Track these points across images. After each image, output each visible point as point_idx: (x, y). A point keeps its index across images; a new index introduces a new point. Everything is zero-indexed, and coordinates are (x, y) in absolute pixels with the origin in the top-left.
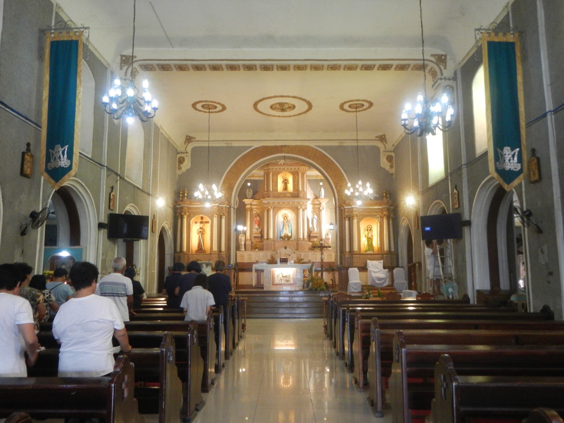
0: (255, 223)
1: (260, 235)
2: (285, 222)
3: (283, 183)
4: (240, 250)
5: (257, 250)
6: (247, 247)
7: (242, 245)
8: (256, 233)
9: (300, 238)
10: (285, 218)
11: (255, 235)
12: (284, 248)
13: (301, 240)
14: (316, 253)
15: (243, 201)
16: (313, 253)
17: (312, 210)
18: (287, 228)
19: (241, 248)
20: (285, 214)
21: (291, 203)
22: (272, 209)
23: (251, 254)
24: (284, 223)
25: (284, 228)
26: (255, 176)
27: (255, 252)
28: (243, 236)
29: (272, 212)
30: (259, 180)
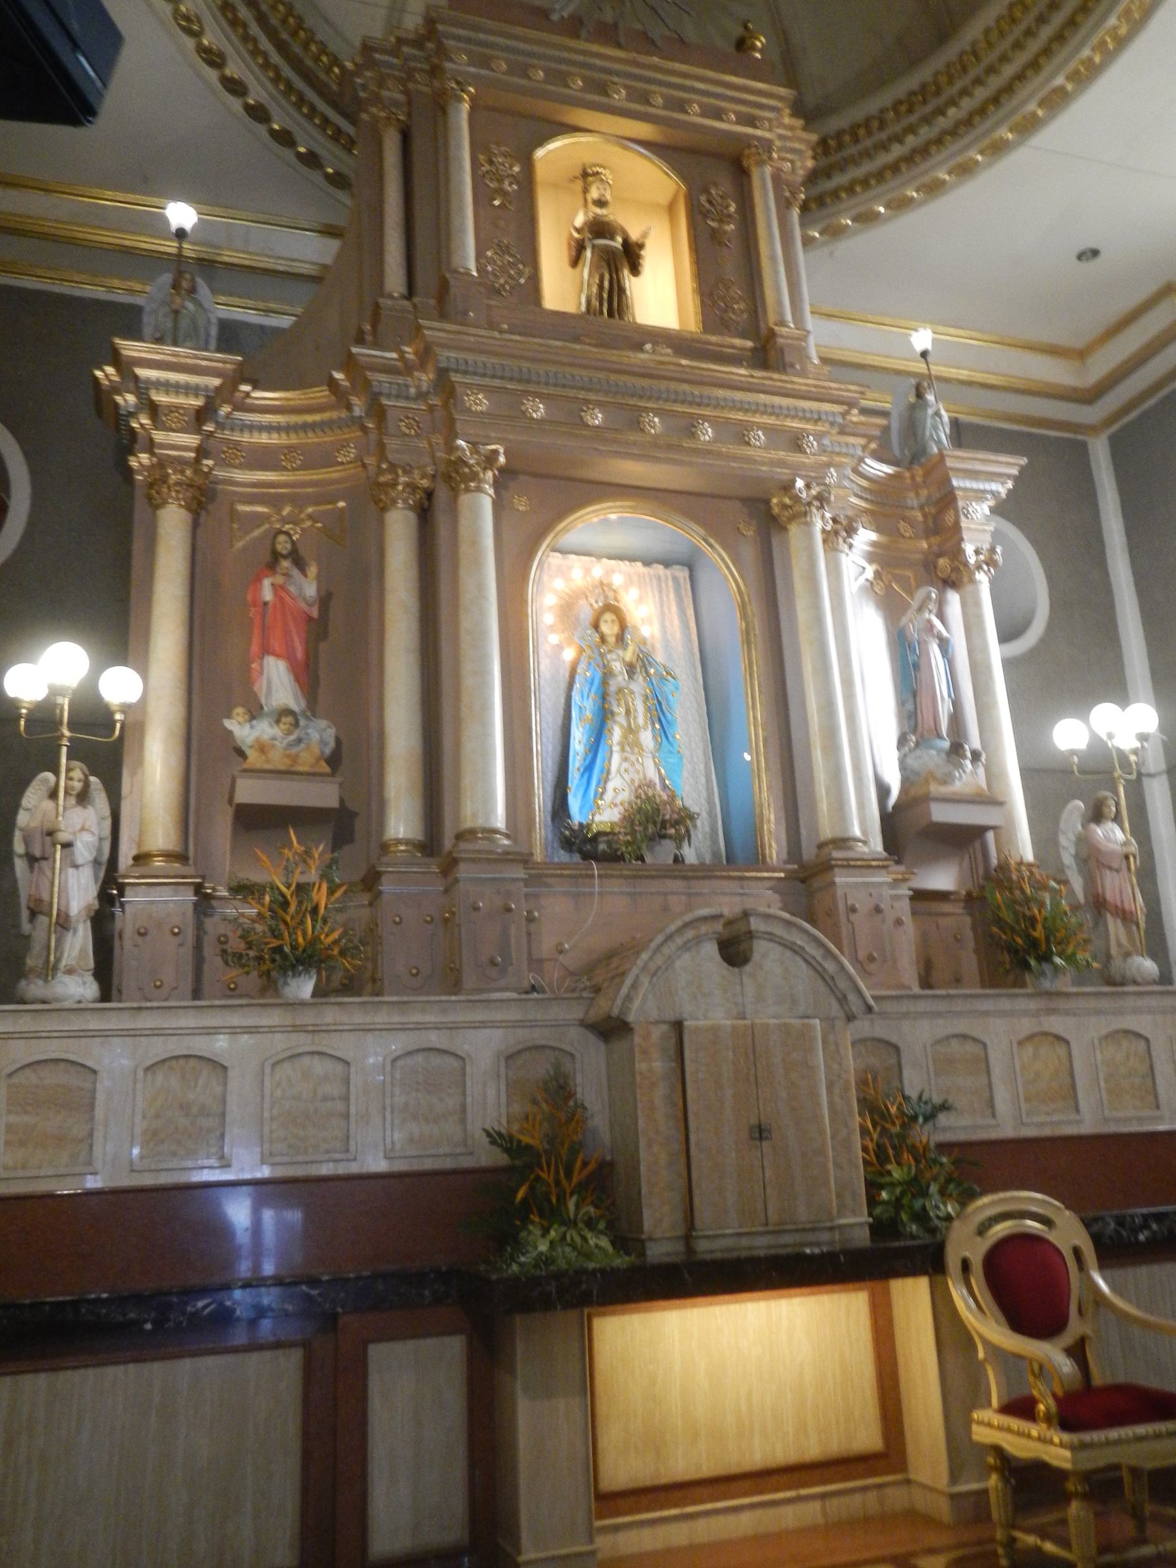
0: (266, 650)
1: (325, 795)
2: (617, 666)
3: (575, 261)
4: (34, 988)
5: (304, 987)
6: (127, 952)
7: (64, 924)
8: (277, 760)
9: (843, 842)
10: (609, 628)
11: (250, 792)
12: (711, 949)
13: (865, 865)
14: (1055, 1024)
15: (107, 374)
16: (1026, 1026)
17: (870, 572)
18: (647, 738)
19: (49, 970)
20: (603, 586)
21: (707, 433)
22: (489, 475)
23: (199, 1045)
24: (607, 675)
25: (617, 734)
26: (228, 256)
27: (273, 1018)
28: (83, 798)
29: (486, 503)
30: (262, 328)
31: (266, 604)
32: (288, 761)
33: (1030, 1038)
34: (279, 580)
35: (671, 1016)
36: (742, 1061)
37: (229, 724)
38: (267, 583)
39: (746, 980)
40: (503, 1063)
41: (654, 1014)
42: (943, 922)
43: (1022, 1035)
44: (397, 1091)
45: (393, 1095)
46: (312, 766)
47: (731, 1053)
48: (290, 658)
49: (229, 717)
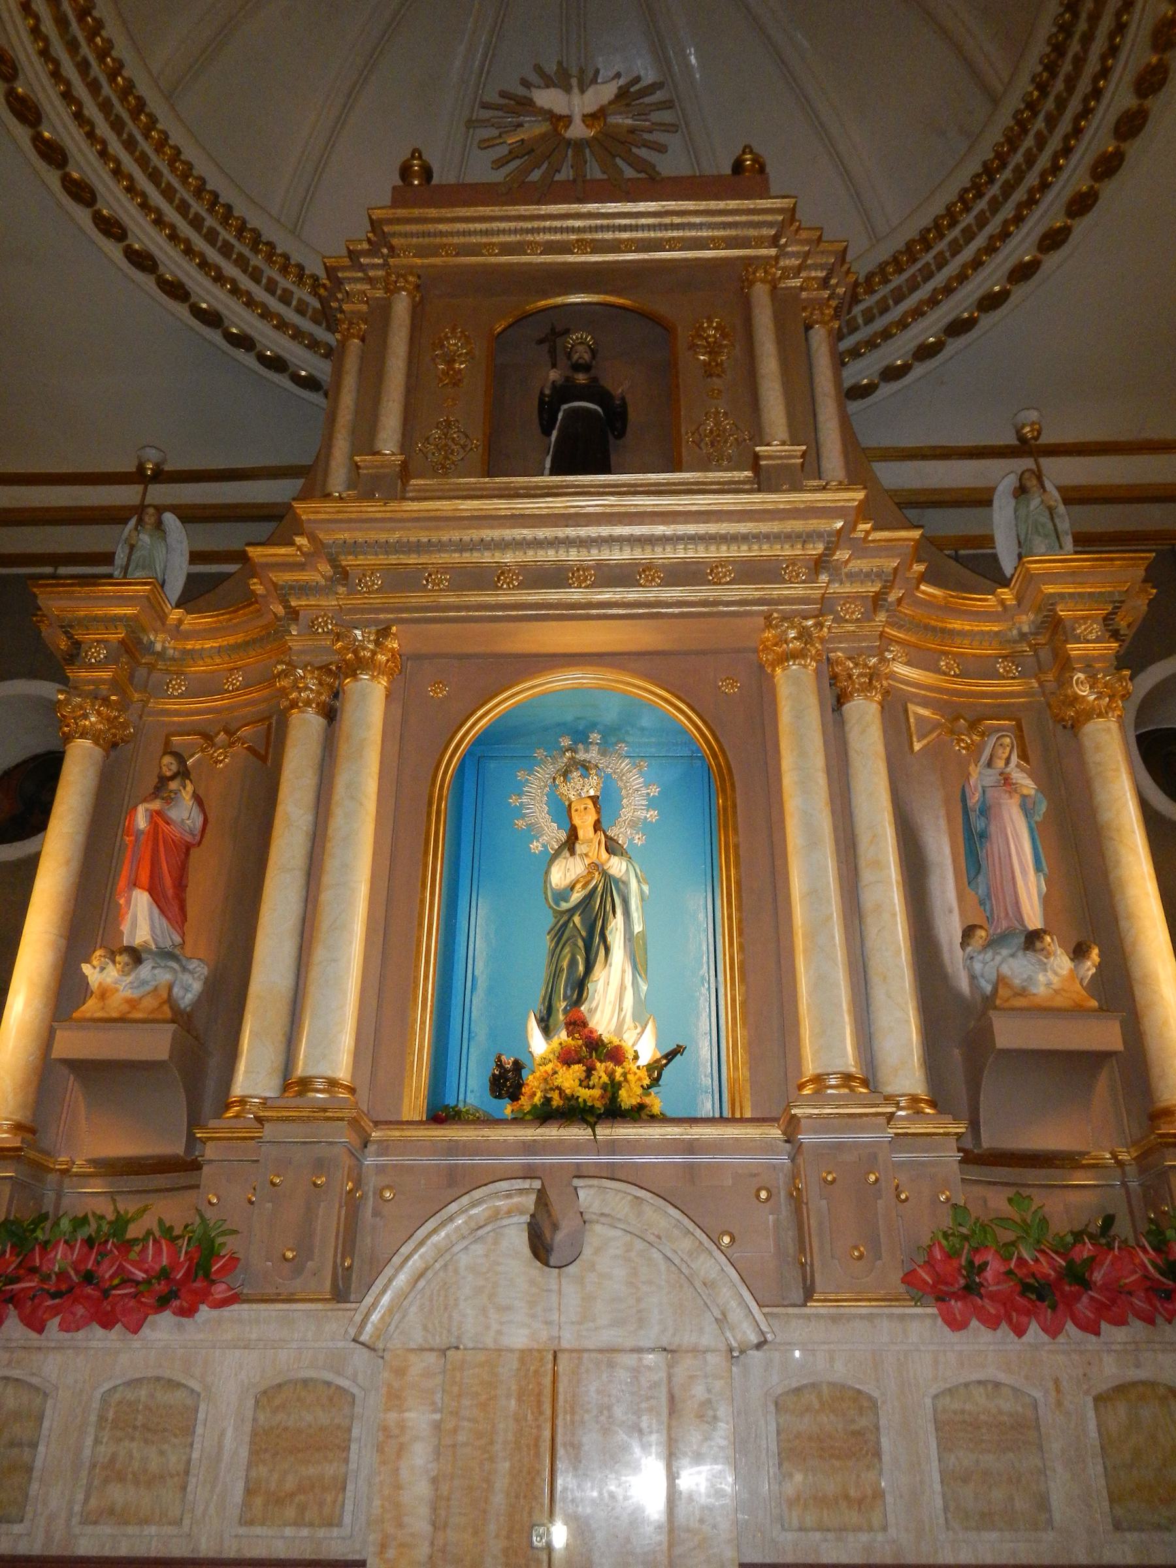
0: (135, 884)
12: (517, 1238)
31: (140, 833)
32: (125, 1008)
33: (1121, 1389)
34: (156, 805)
35: (438, 1341)
36: (530, 1417)
37: (86, 969)
38: (141, 810)
39: (569, 1288)
40: (251, 1402)
41: (417, 1338)
42: (1074, 1197)
43: (1102, 1387)
44: (105, 1436)
45: (97, 1441)
46: (152, 1012)
47: (513, 1402)
48: (152, 891)
49: (88, 961)
